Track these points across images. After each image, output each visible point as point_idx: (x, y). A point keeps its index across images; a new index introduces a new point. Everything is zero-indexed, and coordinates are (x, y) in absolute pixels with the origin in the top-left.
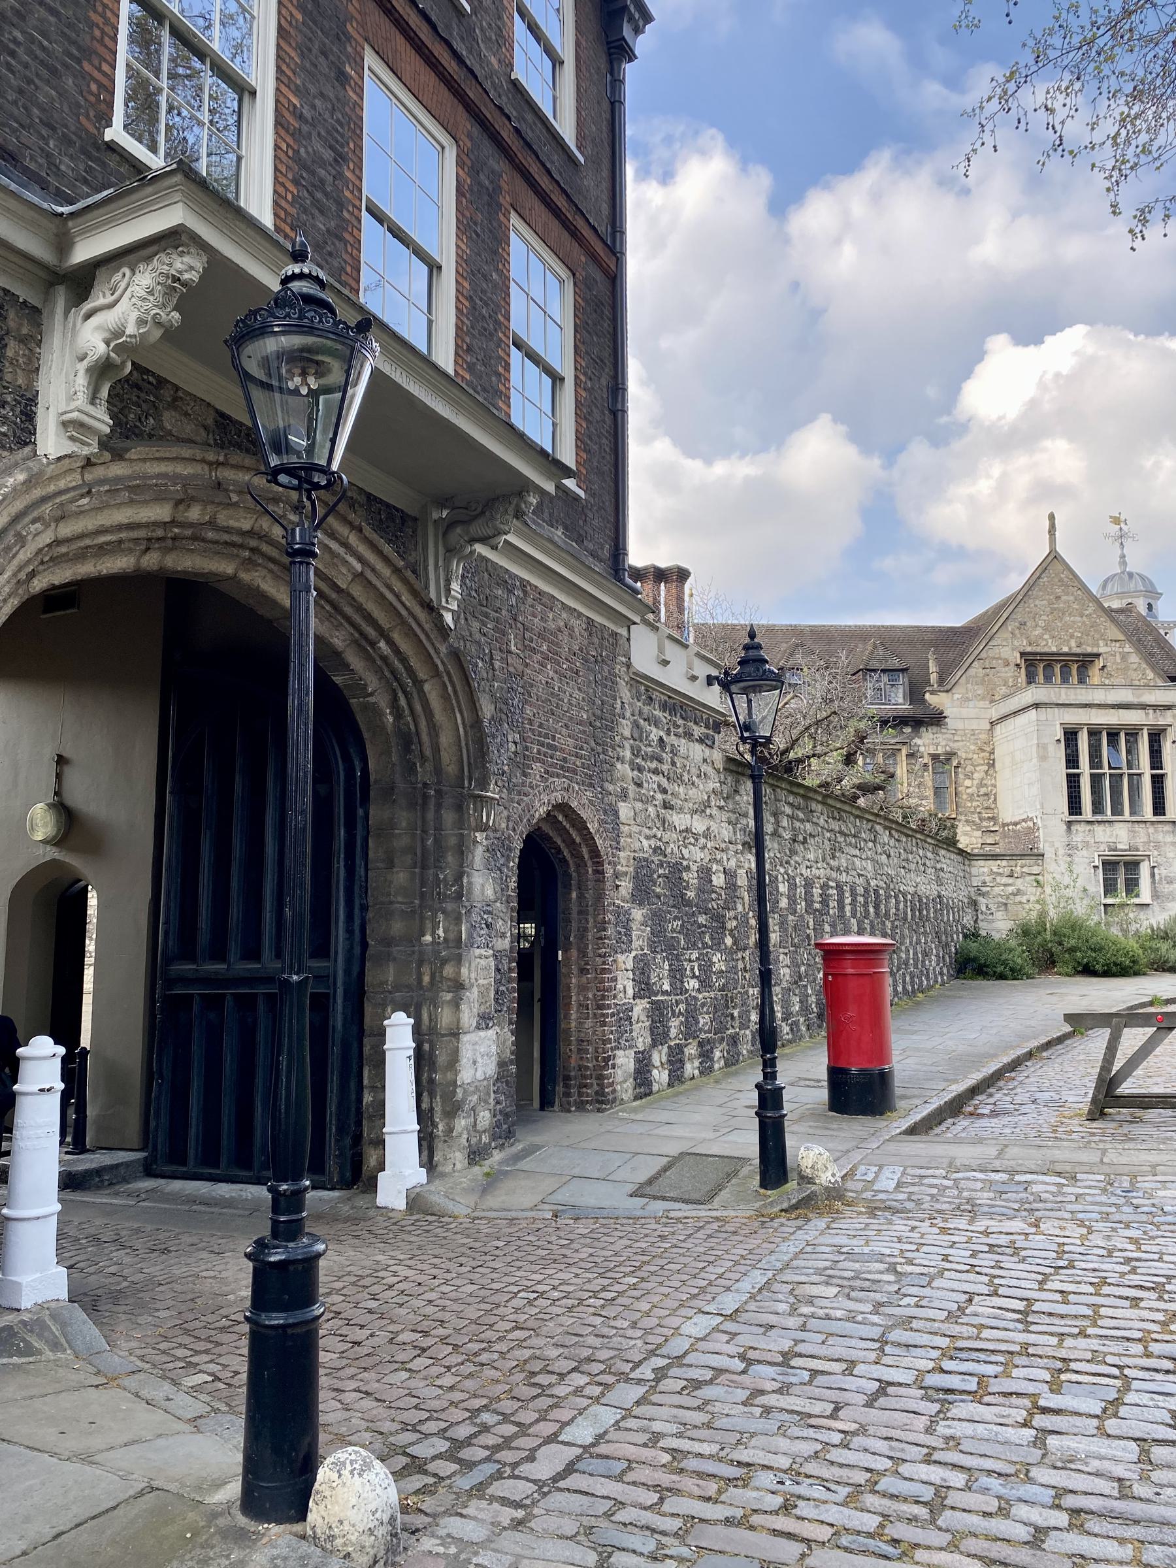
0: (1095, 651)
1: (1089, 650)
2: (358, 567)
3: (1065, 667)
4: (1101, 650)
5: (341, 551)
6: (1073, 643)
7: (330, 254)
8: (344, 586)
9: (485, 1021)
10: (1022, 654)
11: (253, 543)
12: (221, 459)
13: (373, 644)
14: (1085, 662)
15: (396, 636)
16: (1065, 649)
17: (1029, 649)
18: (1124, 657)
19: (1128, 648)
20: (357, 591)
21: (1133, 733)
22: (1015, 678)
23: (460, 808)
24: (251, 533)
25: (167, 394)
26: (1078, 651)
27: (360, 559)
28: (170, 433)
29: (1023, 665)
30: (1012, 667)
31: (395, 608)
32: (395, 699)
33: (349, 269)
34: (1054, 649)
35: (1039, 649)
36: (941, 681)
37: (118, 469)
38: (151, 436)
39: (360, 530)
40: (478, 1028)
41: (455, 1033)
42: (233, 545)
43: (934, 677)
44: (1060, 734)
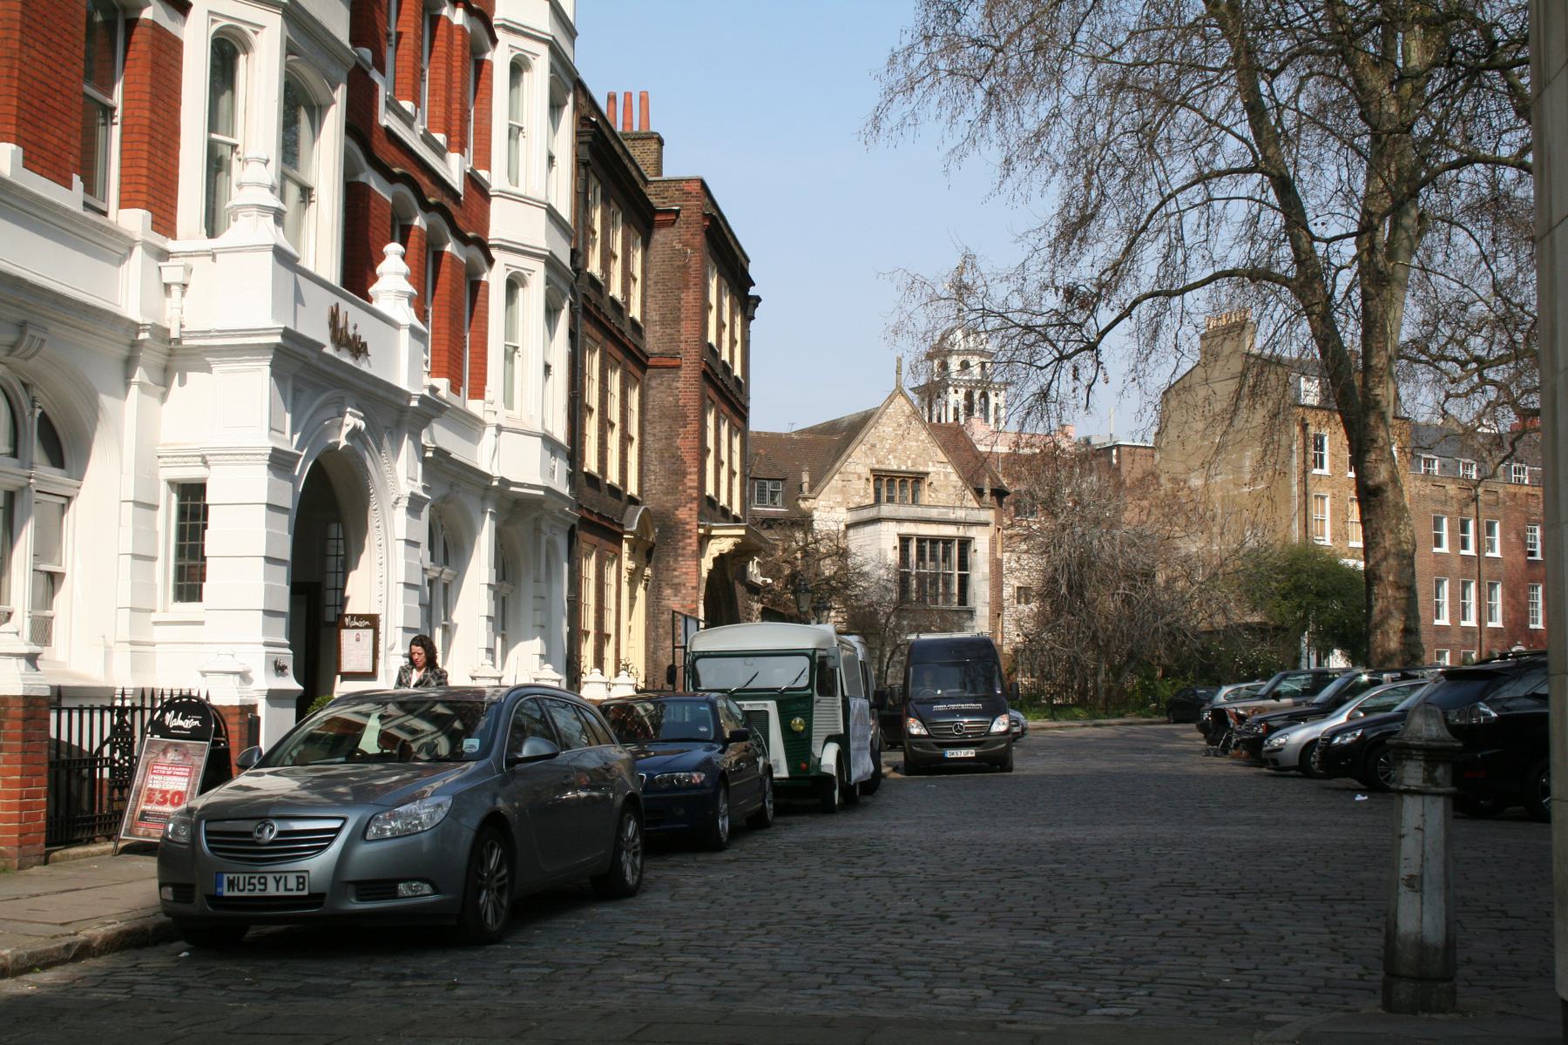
0: (925, 470)
1: (921, 469)
3: (904, 481)
4: (930, 470)
6: (909, 464)
10: (872, 470)
14: (919, 478)
16: (904, 468)
17: (877, 467)
18: (946, 475)
19: (950, 469)
21: (947, 541)
22: (865, 490)
26: (914, 469)
29: (872, 479)
30: (864, 481)
34: (895, 468)
35: (883, 467)
36: (811, 489)
43: (806, 487)
44: (897, 543)
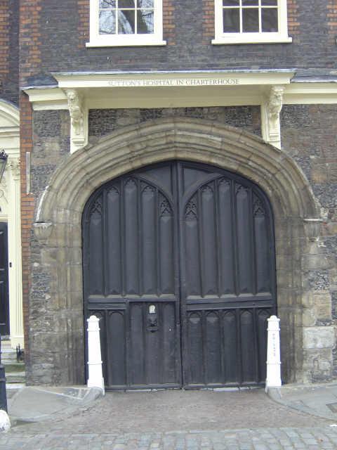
2: (220, 139)
5: (209, 136)
7: (195, 21)
8: (219, 147)
9: (323, 322)
11: (170, 146)
12: (138, 127)
13: (247, 164)
15: (253, 158)
20: (227, 148)
23: (301, 227)
24: (167, 143)
25: (118, 114)
27: (219, 136)
28: (121, 126)
31: (244, 149)
32: (268, 183)
33: (206, 21)
37: (98, 148)
38: (113, 130)
39: (214, 126)
40: (317, 325)
41: (301, 326)
42: (163, 149)
